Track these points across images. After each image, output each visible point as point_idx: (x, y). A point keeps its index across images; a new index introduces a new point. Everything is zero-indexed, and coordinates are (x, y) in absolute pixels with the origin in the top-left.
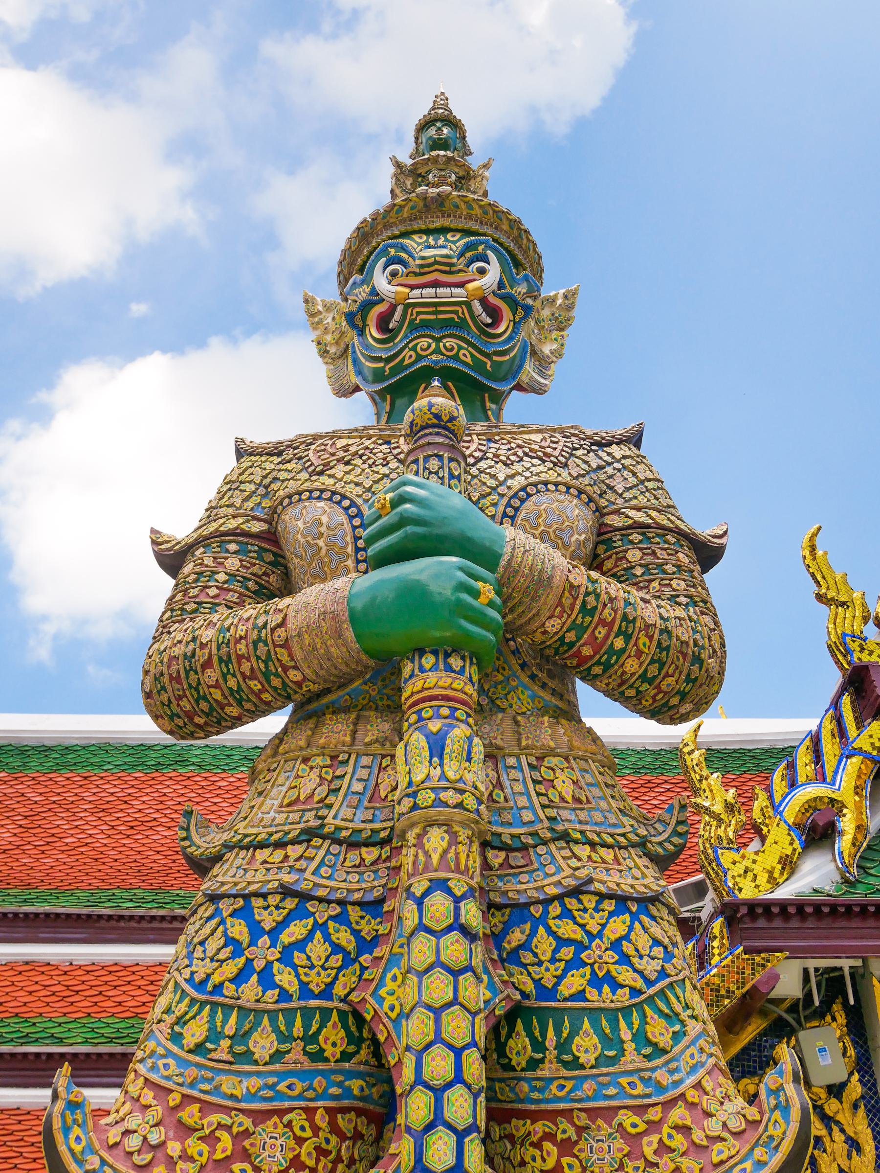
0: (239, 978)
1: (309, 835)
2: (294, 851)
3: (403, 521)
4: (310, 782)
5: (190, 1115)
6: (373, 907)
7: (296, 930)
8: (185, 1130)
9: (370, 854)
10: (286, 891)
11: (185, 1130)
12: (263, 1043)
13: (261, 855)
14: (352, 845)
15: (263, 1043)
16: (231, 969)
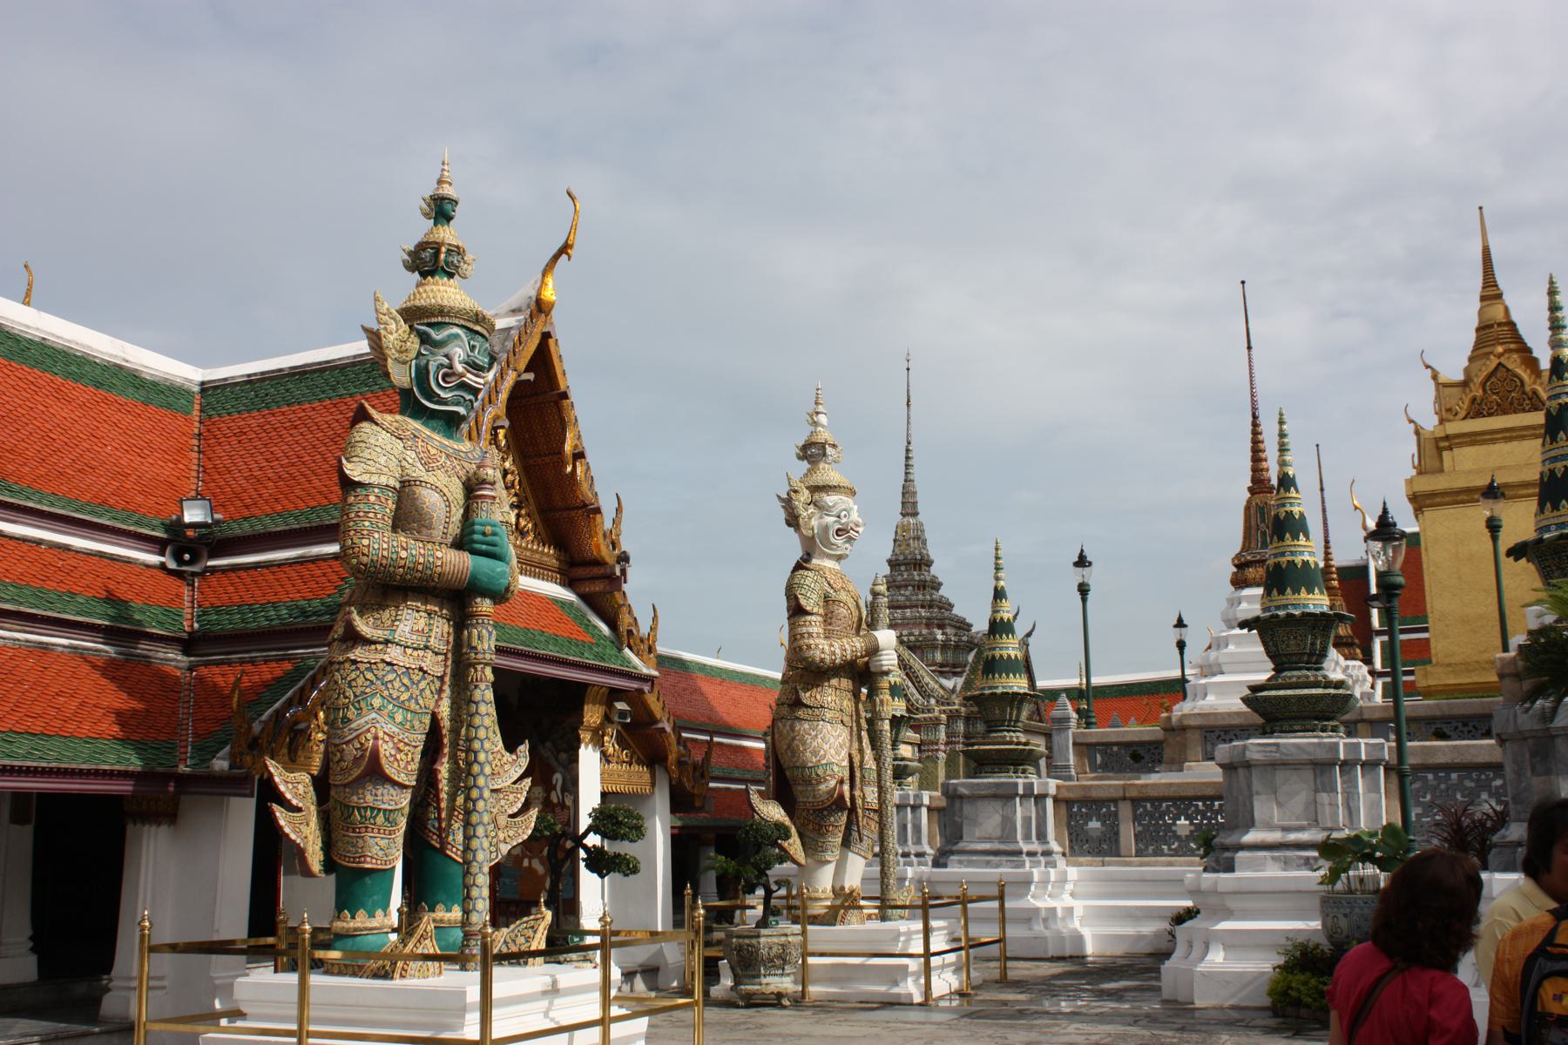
0: (409, 700)
1: (426, 647)
2: (421, 653)
3: (494, 545)
4: (422, 623)
5: (401, 745)
6: (441, 678)
7: (423, 684)
8: (400, 751)
9: (441, 658)
10: (421, 669)
11: (400, 751)
12: (417, 723)
13: (409, 651)
14: (436, 654)
15: (417, 723)
16: (405, 696)
